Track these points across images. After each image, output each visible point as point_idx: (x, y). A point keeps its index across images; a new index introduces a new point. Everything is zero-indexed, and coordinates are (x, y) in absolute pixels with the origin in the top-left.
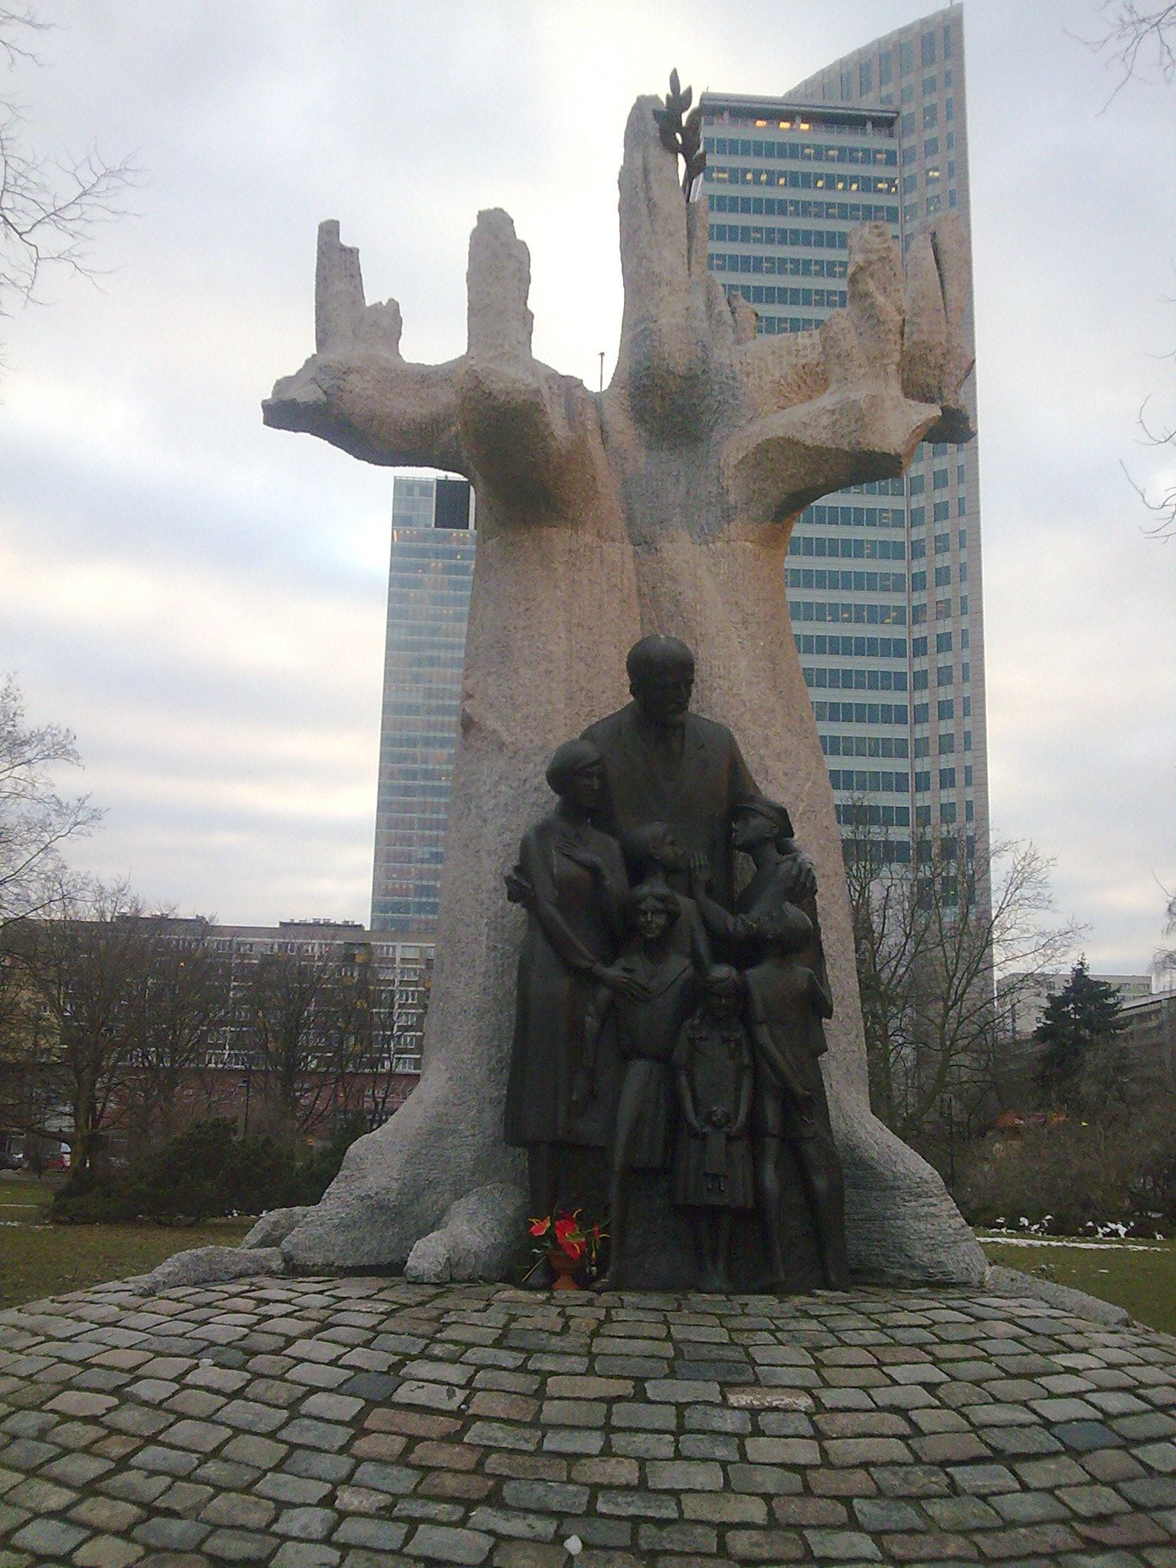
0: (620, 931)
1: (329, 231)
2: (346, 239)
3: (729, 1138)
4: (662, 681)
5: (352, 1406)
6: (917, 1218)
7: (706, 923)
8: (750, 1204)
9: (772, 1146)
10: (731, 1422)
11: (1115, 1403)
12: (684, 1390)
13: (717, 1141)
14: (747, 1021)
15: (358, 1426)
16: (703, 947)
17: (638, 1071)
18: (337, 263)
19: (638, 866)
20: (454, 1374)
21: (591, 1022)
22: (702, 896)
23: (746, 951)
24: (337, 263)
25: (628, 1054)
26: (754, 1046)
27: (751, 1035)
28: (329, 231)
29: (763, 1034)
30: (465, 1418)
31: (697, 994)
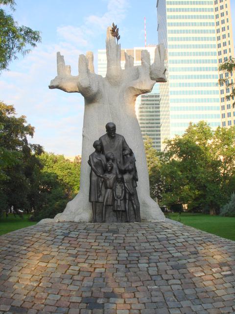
0: (105, 170)
1: (58, 53)
2: (61, 54)
3: (121, 200)
4: (111, 130)
5: (62, 237)
6: (154, 211)
7: (119, 169)
8: (124, 209)
9: (127, 201)
10: (112, 238)
11: (169, 235)
12: (107, 234)
13: (119, 200)
14: (124, 183)
15: (63, 239)
16: (118, 171)
17: (109, 191)
18: (60, 58)
19: (108, 159)
20: (77, 233)
21: (101, 184)
22: (118, 163)
23: (123, 172)
24: (60, 58)
25: (106, 188)
26: (125, 186)
27: (124, 185)
28: (58, 53)
29: (126, 184)
30: (77, 238)
31: (117, 180)
